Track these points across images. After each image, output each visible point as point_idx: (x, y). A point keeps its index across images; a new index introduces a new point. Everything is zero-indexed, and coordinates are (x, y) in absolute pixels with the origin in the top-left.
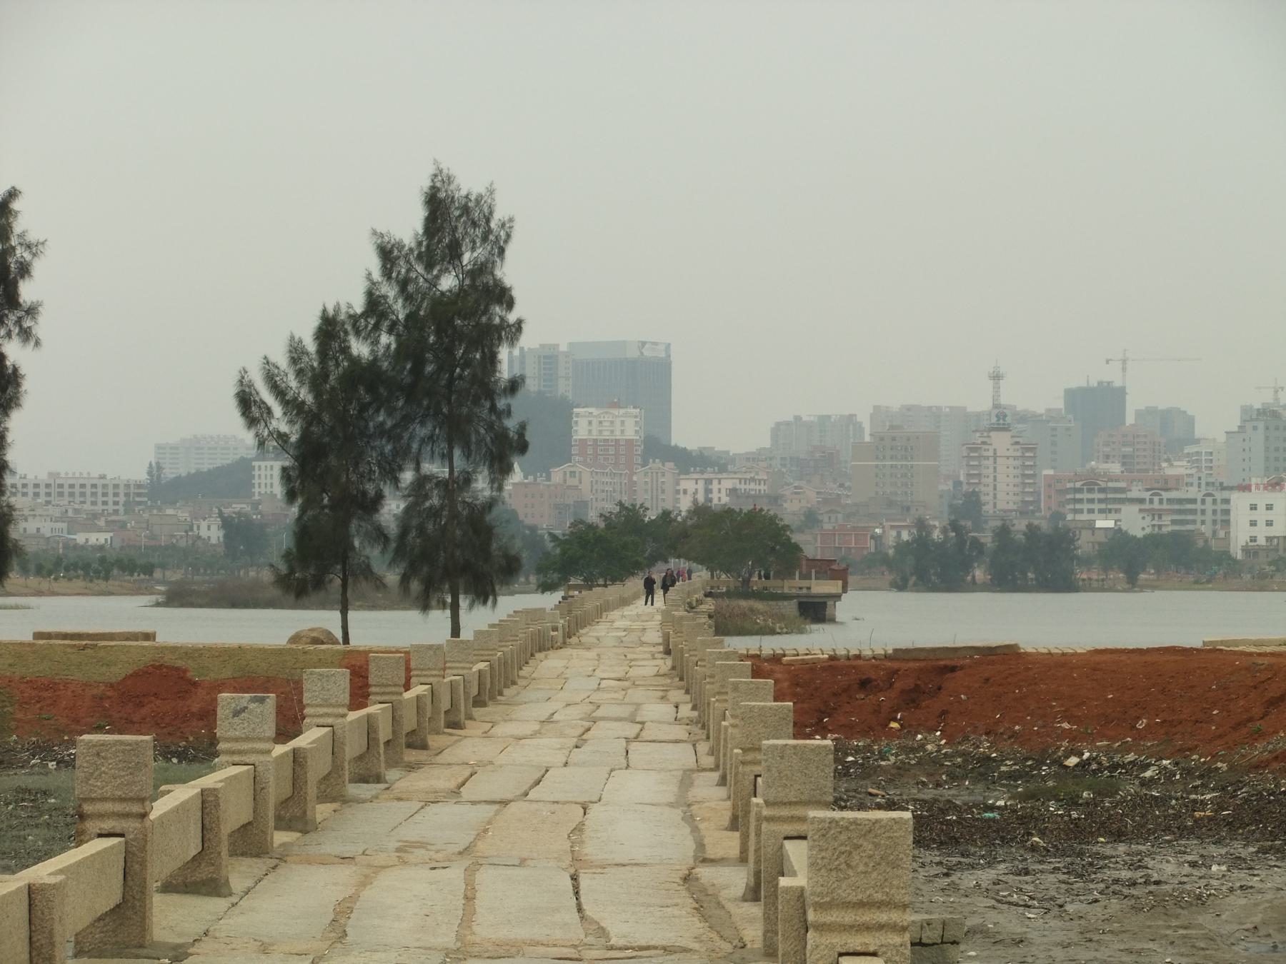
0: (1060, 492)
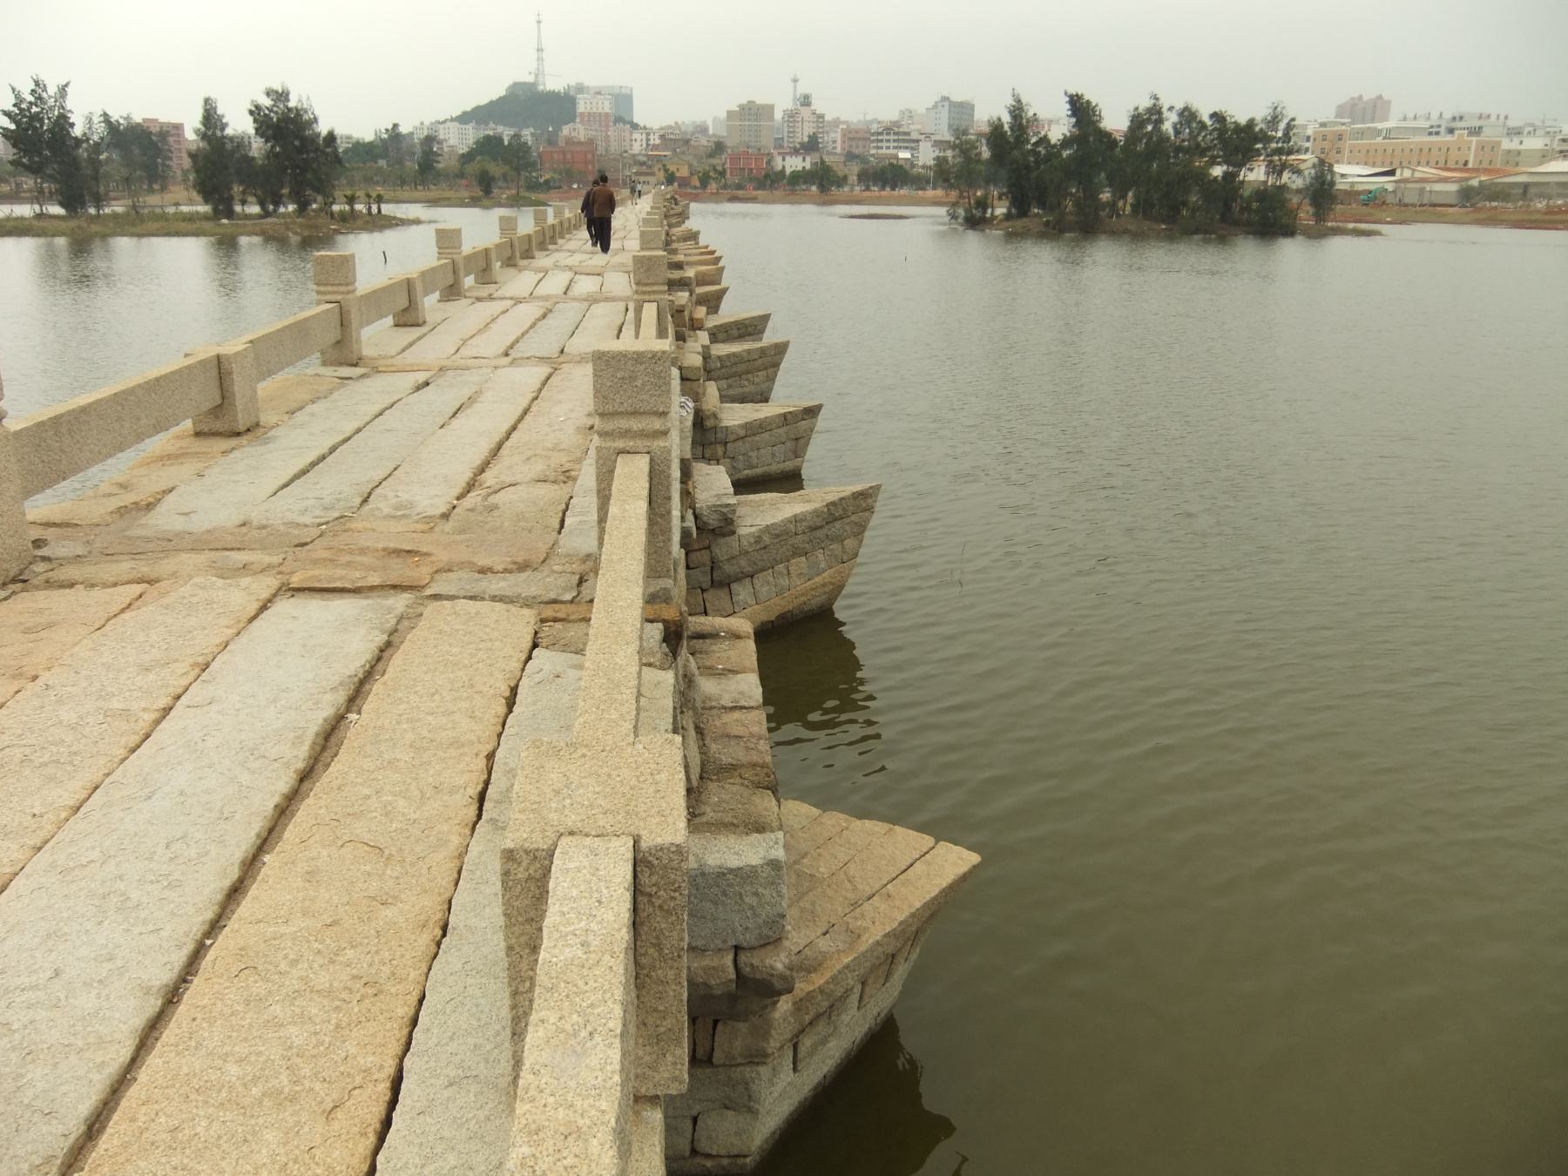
0: (849, 139)
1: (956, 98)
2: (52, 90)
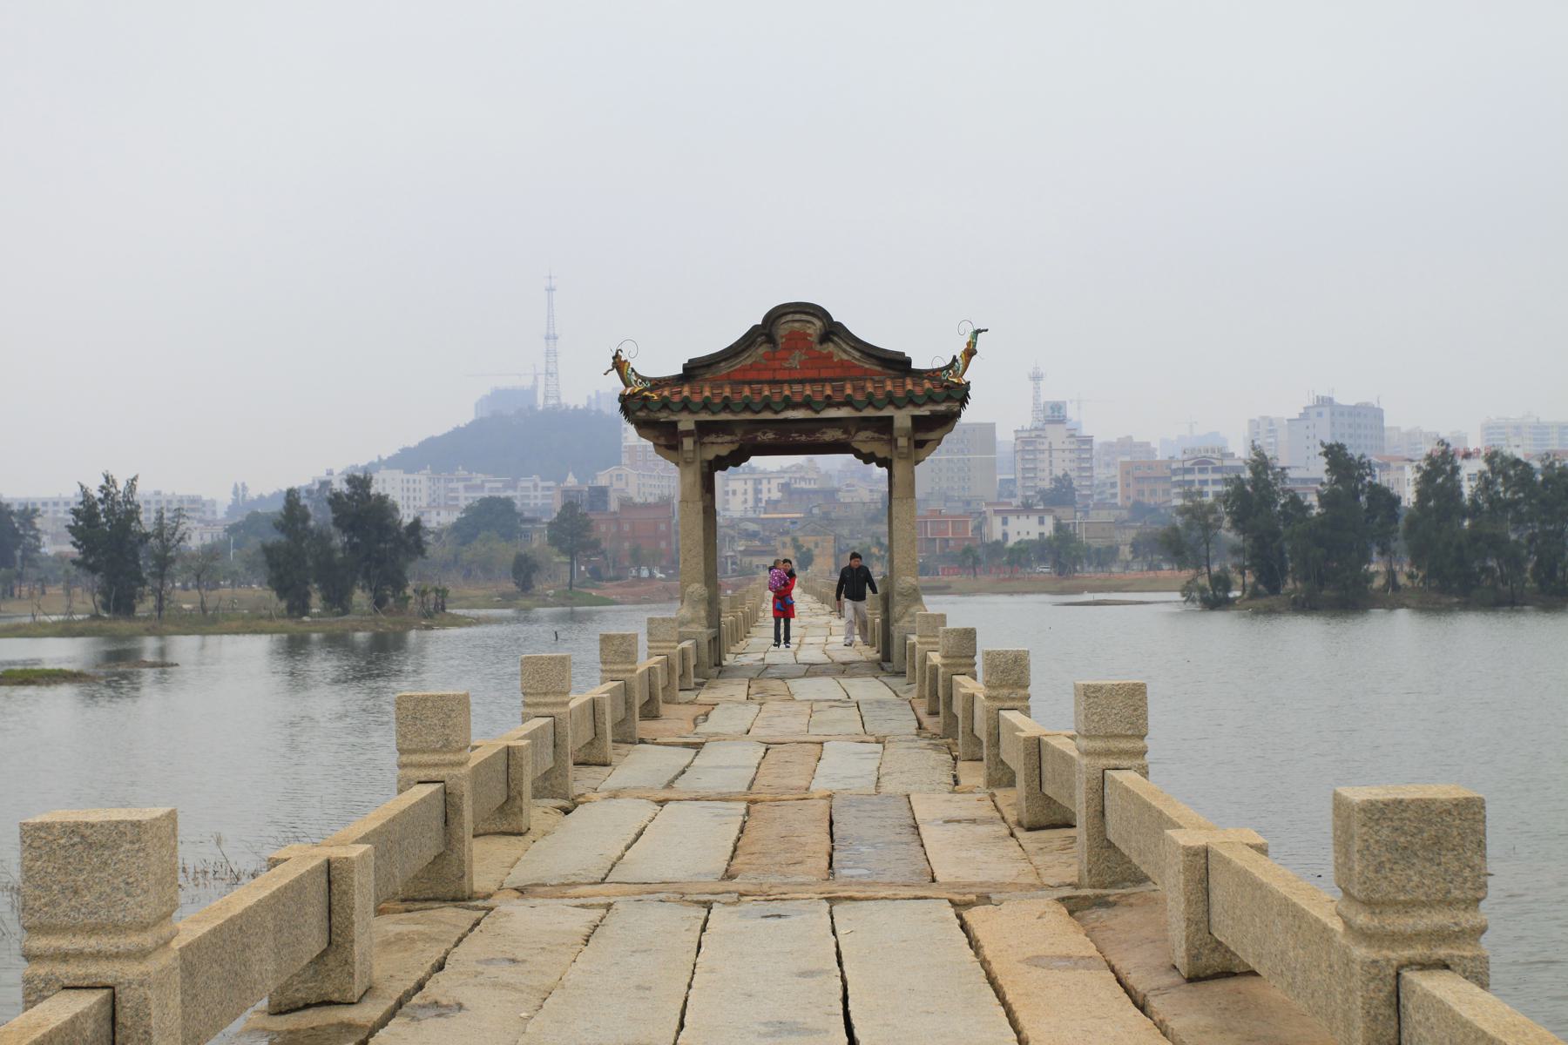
0: (1138, 479)
1: (1345, 398)
2: (121, 486)
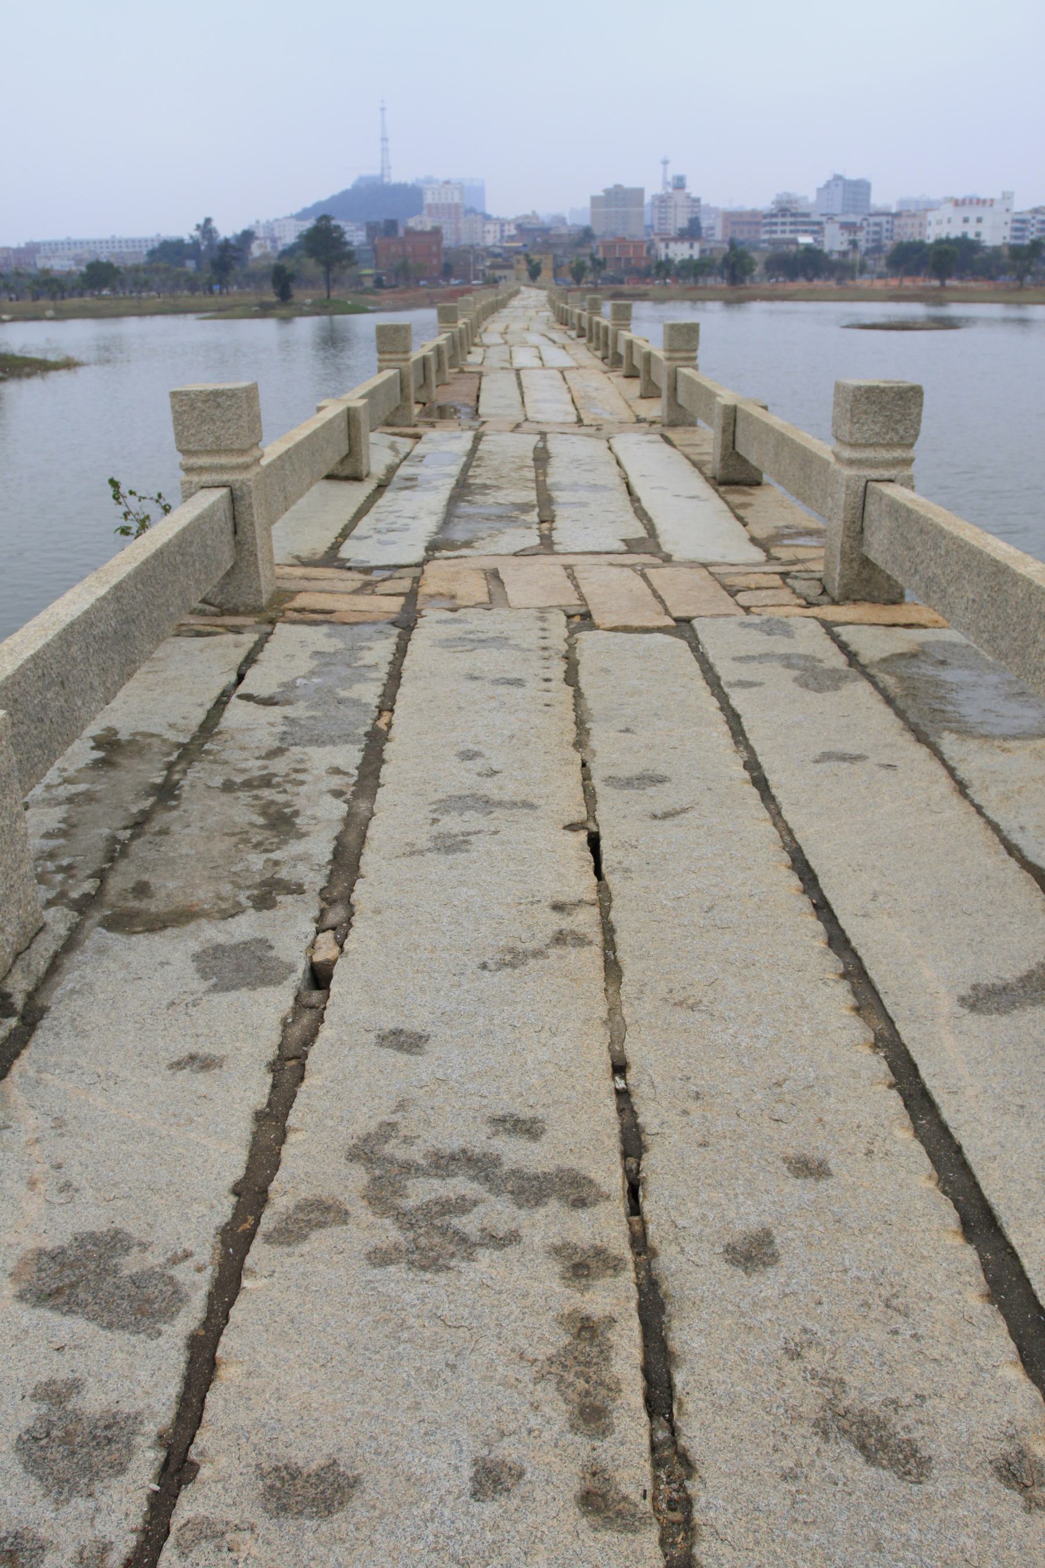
1: (851, 176)
